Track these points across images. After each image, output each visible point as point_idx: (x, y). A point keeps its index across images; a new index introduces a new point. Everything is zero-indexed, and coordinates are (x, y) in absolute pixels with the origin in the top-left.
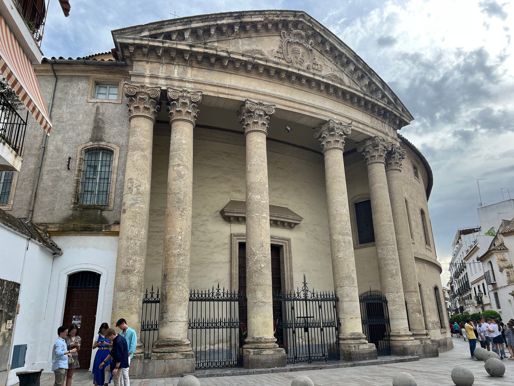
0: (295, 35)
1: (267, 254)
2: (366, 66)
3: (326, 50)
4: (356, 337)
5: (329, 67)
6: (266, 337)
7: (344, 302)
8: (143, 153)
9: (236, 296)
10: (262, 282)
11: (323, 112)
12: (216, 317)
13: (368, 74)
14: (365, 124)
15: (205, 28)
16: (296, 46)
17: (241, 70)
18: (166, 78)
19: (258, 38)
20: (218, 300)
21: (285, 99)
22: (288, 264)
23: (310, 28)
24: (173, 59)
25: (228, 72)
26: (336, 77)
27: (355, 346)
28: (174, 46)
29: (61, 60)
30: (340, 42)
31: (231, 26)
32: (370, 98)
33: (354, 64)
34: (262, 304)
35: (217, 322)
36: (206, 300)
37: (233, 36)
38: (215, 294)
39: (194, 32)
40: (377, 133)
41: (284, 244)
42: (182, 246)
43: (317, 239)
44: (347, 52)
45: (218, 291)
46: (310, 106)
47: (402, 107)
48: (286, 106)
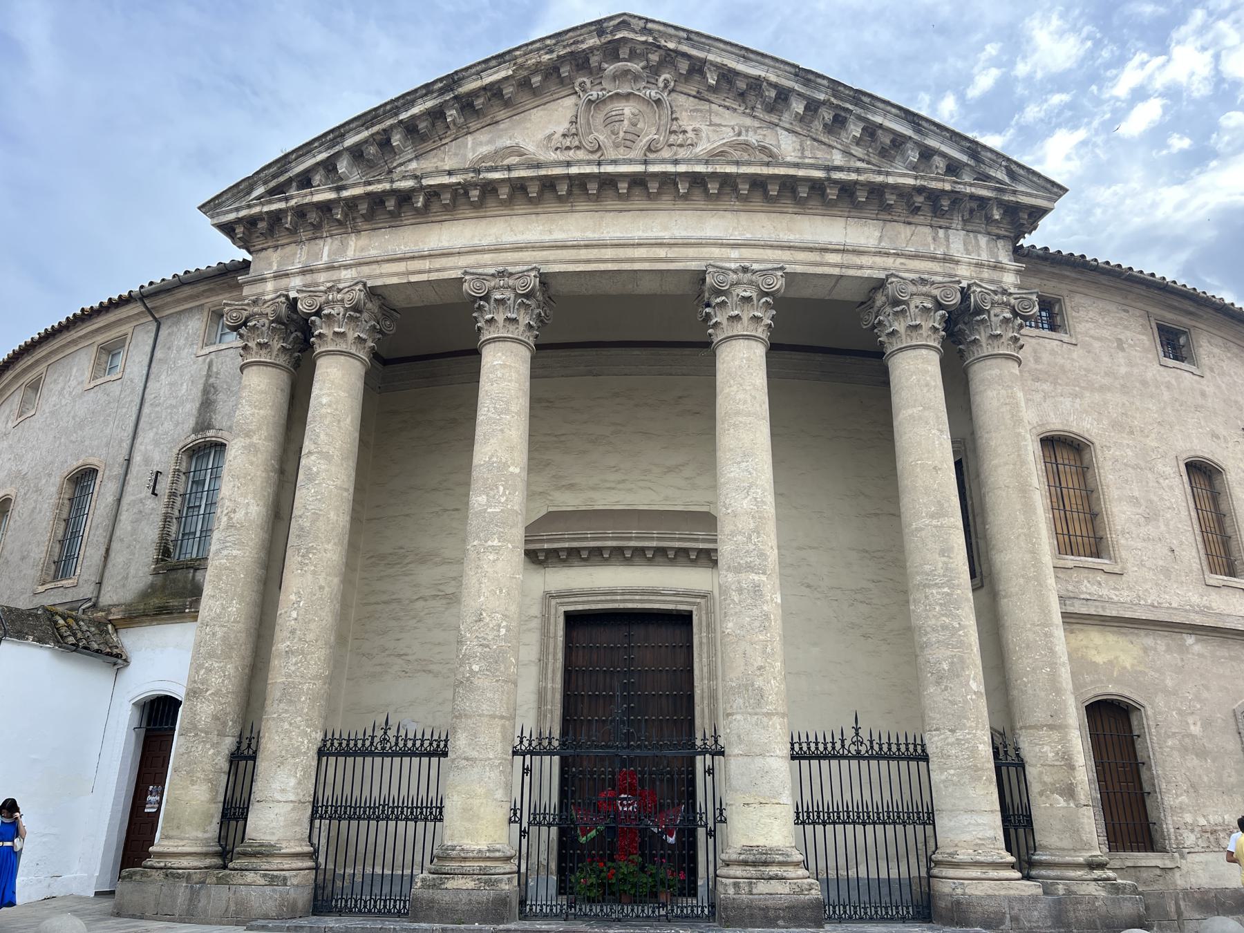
0: (615, 78)
1: (490, 637)
2: (841, 89)
3: (709, 86)
4: (751, 858)
5: (725, 126)
6: (467, 844)
7: (732, 758)
8: (248, 441)
9: (556, 743)
10: (471, 708)
11: (691, 252)
12: (376, 793)
13: (851, 107)
14: (848, 250)
15: (378, 137)
16: (616, 105)
17: (462, 208)
18: (304, 272)
19: (514, 117)
20: (383, 754)
21: (573, 247)
22: (705, 660)
23: (650, 47)
24: (317, 227)
25: (433, 219)
26: (746, 146)
27: (739, 883)
28: (307, 200)
29: (153, 286)
30: (743, 52)
31: (437, 114)
32: (853, 174)
33: (799, 94)
34: (464, 763)
35: (377, 805)
36: (355, 754)
37: (451, 135)
38: (376, 740)
39: (357, 153)
40: (902, 264)
41: (694, 609)
42: (298, 632)
43: (809, 586)
44: (771, 69)
45: (385, 733)
46: (646, 244)
47: (1006, 167)
48: (579, 262)
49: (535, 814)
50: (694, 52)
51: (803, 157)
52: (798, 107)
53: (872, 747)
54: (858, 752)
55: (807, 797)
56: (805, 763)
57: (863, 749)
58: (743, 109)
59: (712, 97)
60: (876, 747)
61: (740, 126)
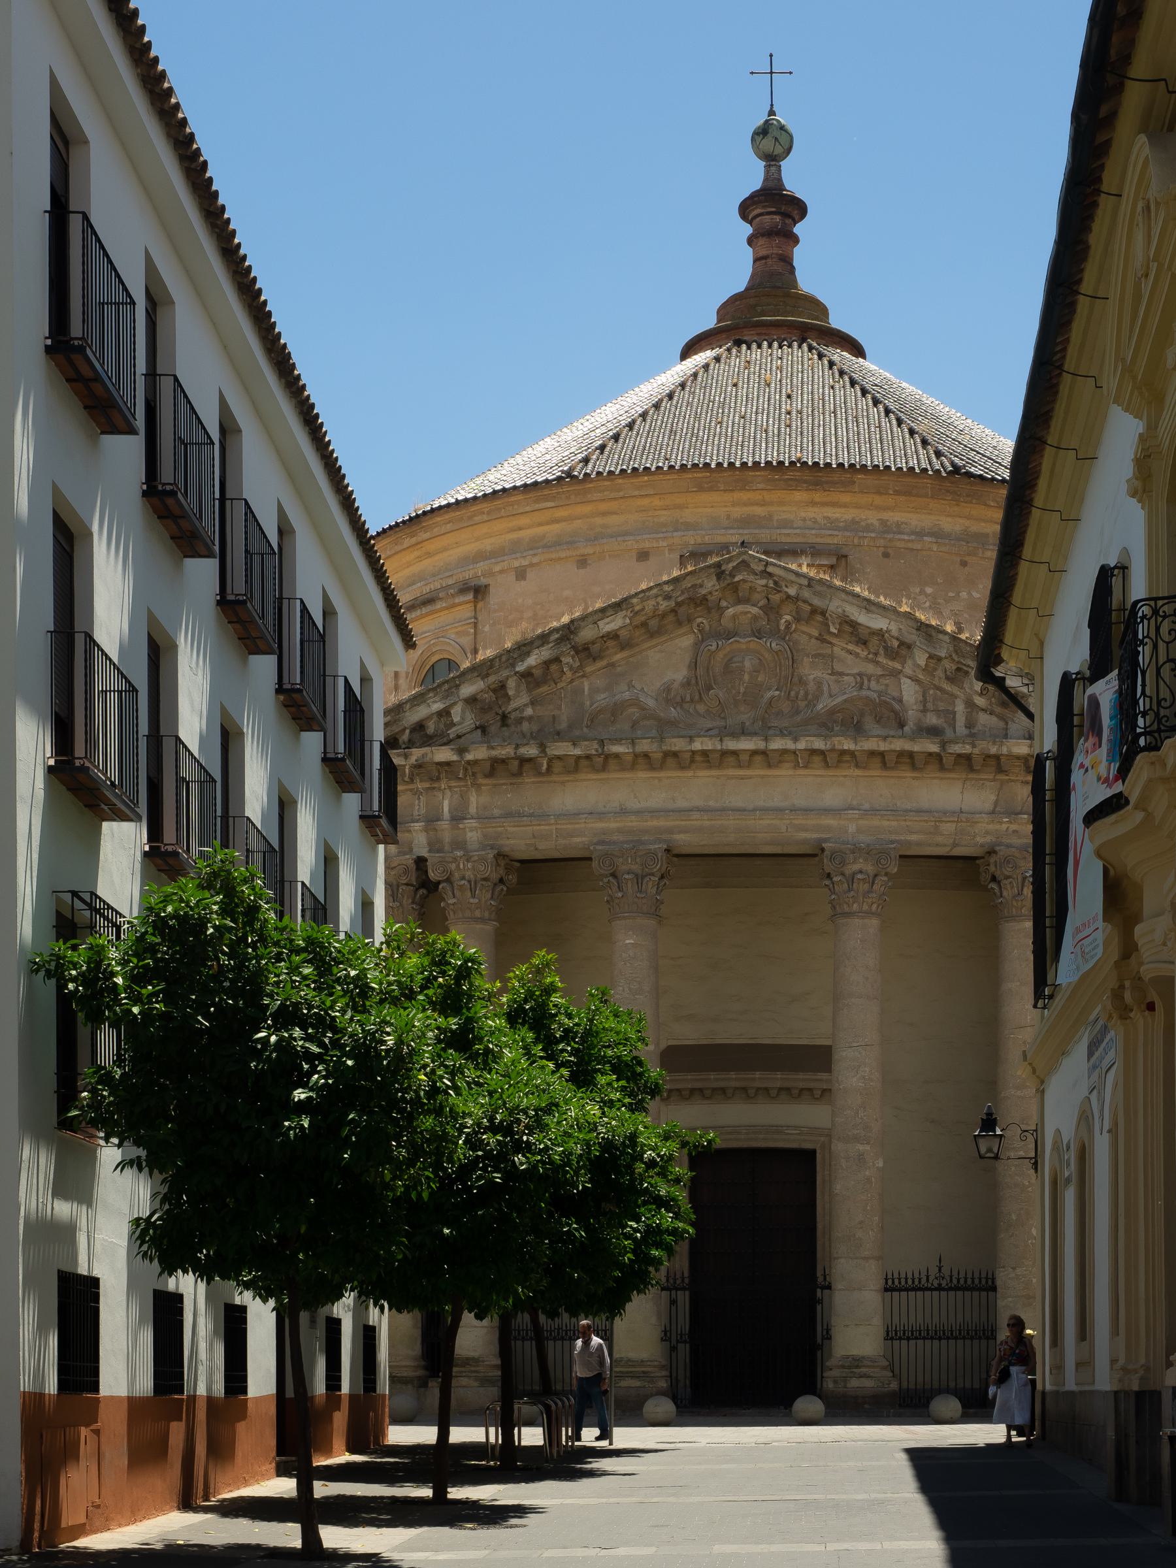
5: (848, 675)
49: (681, 1335)
50: (816, 601)
51: (924, 711)
52: (921, 659)
53: (951, 1281)
54: (940, 1285)
55: (896, 1320)
56: (896, 1294)
57: (944, 1283)
58: (865, 653)
59: (834, 640)
60: (955, 1281)
61: (860, 675)
